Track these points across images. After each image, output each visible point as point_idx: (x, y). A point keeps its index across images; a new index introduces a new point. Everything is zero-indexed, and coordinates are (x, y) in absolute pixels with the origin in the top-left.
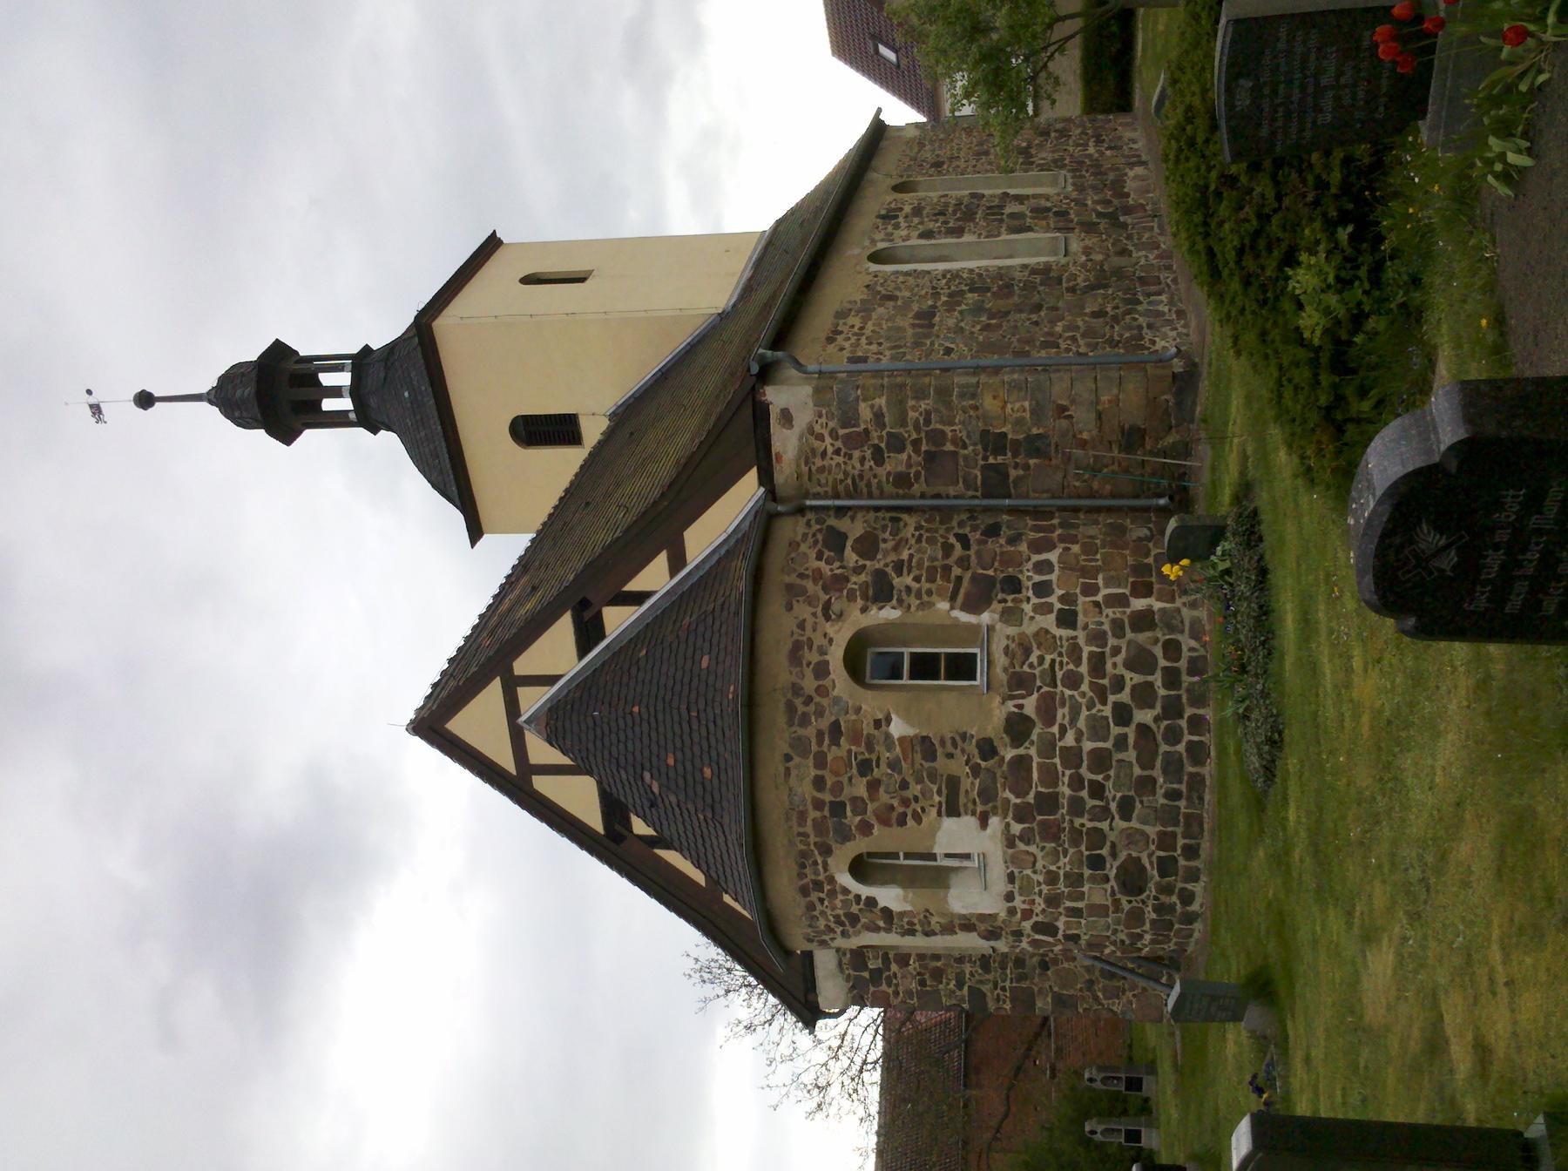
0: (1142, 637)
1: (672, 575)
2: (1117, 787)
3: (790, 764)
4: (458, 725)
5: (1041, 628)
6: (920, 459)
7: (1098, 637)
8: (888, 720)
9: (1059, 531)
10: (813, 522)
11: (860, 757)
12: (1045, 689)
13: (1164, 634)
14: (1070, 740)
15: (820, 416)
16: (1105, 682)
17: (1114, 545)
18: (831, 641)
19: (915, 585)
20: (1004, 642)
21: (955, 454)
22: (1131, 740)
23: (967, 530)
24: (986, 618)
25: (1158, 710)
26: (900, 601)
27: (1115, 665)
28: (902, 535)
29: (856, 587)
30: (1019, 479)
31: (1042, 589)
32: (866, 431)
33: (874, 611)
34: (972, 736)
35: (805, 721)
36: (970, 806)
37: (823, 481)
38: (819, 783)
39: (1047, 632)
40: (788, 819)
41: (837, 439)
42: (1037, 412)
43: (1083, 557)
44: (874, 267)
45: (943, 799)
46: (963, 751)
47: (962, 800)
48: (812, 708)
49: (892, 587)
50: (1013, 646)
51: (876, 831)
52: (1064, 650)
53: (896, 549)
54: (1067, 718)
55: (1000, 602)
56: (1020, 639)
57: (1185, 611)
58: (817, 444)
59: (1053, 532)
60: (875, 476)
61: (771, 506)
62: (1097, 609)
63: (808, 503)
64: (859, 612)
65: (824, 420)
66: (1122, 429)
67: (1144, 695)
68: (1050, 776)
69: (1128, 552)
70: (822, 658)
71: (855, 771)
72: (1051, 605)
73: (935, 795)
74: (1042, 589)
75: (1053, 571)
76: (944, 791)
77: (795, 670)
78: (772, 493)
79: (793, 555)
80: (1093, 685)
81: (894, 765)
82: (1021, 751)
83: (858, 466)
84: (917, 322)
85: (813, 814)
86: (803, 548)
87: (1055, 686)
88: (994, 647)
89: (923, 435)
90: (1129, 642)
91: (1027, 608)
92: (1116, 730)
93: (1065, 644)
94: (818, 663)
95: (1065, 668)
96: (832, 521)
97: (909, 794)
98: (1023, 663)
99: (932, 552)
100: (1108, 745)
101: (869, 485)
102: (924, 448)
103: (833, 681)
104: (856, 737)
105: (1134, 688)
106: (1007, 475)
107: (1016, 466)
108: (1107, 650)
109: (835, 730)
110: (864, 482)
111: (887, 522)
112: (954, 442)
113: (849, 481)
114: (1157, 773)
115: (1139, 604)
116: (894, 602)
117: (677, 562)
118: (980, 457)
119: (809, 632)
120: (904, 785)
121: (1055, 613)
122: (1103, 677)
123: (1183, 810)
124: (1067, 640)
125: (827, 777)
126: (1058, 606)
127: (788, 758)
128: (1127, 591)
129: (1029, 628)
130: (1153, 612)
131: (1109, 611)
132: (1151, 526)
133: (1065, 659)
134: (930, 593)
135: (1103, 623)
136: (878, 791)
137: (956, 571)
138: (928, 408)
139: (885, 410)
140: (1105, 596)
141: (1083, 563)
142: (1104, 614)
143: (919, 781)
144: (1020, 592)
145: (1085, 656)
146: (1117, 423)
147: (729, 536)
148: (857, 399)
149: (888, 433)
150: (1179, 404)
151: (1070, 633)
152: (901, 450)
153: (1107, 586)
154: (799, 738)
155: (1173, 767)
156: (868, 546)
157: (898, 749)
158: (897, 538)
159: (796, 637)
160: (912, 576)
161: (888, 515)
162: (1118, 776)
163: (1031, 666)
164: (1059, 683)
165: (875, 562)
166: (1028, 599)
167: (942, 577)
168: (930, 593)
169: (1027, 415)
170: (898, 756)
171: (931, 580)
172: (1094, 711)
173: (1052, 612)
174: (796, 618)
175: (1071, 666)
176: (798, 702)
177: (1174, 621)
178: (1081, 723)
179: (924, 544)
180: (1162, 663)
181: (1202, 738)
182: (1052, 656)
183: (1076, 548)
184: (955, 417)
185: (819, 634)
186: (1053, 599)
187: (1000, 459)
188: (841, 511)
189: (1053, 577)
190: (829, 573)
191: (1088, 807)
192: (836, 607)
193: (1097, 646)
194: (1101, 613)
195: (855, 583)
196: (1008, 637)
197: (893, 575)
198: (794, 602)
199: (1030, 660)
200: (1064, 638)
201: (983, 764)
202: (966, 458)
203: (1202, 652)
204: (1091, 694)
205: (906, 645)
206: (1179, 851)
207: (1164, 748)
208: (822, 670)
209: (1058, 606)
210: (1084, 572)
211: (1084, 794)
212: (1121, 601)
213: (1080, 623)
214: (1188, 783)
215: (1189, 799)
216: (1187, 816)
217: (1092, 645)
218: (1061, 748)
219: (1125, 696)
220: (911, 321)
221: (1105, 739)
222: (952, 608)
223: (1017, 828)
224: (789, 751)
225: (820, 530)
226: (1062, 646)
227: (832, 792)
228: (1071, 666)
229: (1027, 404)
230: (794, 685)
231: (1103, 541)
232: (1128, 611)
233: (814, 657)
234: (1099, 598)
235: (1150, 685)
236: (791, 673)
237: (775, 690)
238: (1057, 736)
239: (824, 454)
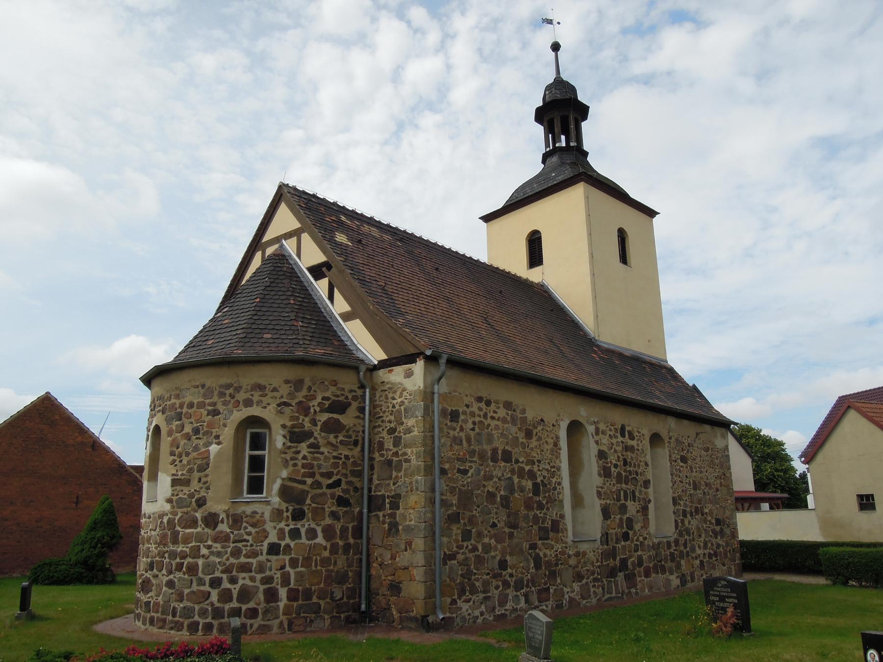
0: (261, 596)
1: (339, 315)
2: (180, 579)
3: (200, 388)
4: (283, 209)
5: (268, 533)
6: (390, 457)
7: (261, 568)
8: (219, 444)
9: (341, 543)
10: (354, 394)
11: (201, 427)
12: (232, 536)
13: (261, 609)
14: (204, 551)
15: (410, 395)
16: (234, 573)
17: (328, 577)
18: (265, 407)
19: (300, 456)
20: (260, 511)
21: (391, 477)
22: (202, 588)
23: (344, 486)
24: (276, 500)
25: (217, 605)
26: (289, 448)
27: (244, 578)
28: (340, 447)
29: (300, 421)
30: (377, 516)
31: (295, 534)
32: (402, 423)
33: (282, 432)
34: (208, 493)
35: (222, 394)
36: (176, 493)
37: (381, 399)
38: (191, 405)
39: (266, 537)
40: (177, 388)
41: (400, 406)
42: (408, 529)
43: (318, 559)
44: (564, 425)
45: (179, 477)
46: (201, 488)
47: (179, 488)
48: (228, 398)
49: (299, 442)
50: (258, 516)
51: (169, 439)
52: (254, 547)
53: (330, 444)
54: (215, 550)
55: (287, 508)
56: (261, 521)
57: (277, 621)
58: (398, 393)
59: (341, 539)
60: (383, 430)
61: (363, 368)
62: (279, 568)
63: (367, 390)
64: (282, 423)
65: (408, 397)
66: (400, 583)
67: (226, 596)
68: (186, 540)
69: (322, 585)
70: (255, 402)
71: (195, 425)
72: (283, 539)
73: (181, 472)
74: (295, 534)
75: (308, 539)
76: (183, 477)
77: (249, 387)
78: (375, 368)
79: (326, 383)
80: (232, 565)
81: (196, 448)
82: (200, 522)
83: (388, 419)
84: (500, 452)
85: (178, 402)
86: (333, 389)
87: (233, 543)
88: (257, 505)
89: (400, 458)
90: (257, 587)
91: (282, 525)
92: (207, 578)
93: (258, 548)
94: (252, 401)
95: (243, 548)
96: (355, 405)
97: (184, 457)
98: (247, 523)
99: (326, 467)
100: (200, 574)
101: (379, 426)
102: (395, 459)
103: (241, 410)
104: (211, 425)
105: (229, 590)
106: (380, 511)
107: (384, 516)
108: (253, 574)
109: (215, 413)
110: (381, 424)
111: (354, 438)
112: (397, 477)
113: (381, 414)
114: (186, 603)
115: (283, 593)
116: (289, 444)
117: (347, 317)
118: (389, 494)
119: (271, 394)
120: (187, 454)
121: (278, 542)
122: (237, 572)
123: (168, 617)
124: (260, 550)
125: (193, 410)
126: (283, 543)
127: (203, 386)
128: (292, 586)
129: (269, 526)
130: (278, 601)
131: (278, 575)
132: (345, 600)
133: (248, 548)
134: (295, 465)
135: (271, 571)
136: (185, 439)
137: (309, 481)
138: (412, 461)
139: (412, 434)
140: (289, 573)
141: (314, 558)
142: (277, 572)
143: (189, 463)
144: (293, 520)
145: (250, 560)
146: (403, 579)
147: (356, 345)
148: (417, 417)
149: (402, 436)
150: (411, 619)
151: (265, 552)
152: (394, 446)
153: (296, 573)
154: (212, 392)
155: (188, 613)
156: (331, 427)
157: (204, 450)
158: (338, 444)
159: (268, 386)
160: (306, 454)
161: (360, 439)
162: (184, 579)
163: (246, 528)
164: (235, 545)
165: (319, 432)
166: (288, 525)
167: (305, 472)
168: (295, 465)
169: (408, 523)
170: (200, 450)
171: (304, 466)
172: (218, 566)
173: (279, 539)
174: (280, 387)
175: (244, 552)
176: (231, 390)
177: (270, 614)
178: (213, 559)
179: (332, 461)
180: (244, 607)
181: (200, 631)
182: (250, 540)
183: (326, 554)
184: (408, 478)
185: (270, 401)
186: (288, 540)
187: (388, 506)
188: (362, 410)
189: (304, 540)
190: (311, 405)
191: (172, 562)
192: (287, 410)
193: (255, 567)
194: (277, 570)
195: (303, 420)
196: (263, 513)
197: (308, 443)
198: (290, 385)
199: (249, 527)
200: (261, 547)
201: (194, 500)
202: (389, 484)
203: (250, 632)
204: (228, 564)
205: (269, 452)
206: (152, 614)
207: (197, 607)
208: (248, 403)
209: (283, 543)
210: (307, 561)
211: (178, 560)
212: (286, 581)
213: (270, 557)
214: (179, 621)
215: (172, 622)
216: (166, 619)
217: (256, 565)
218: (200, 546)
219: (226, 585)
220: (501, 448)
221: (203, 572)
222: (283, 479)
223: (165, 520)
224: (207, 387)
225: (347, 398)
226: (256, 546)
227: (187, 413)
228: (244, 552)
229: (413, 523)
230: (241, 387)
231: (332, 571)
232: (279, 587)
233: (256, 398)
234: (288, 568)
235: (231, 600)
236: (247, 385)
237: (238, 376)
238: (205, 544)
239: (394, 399)
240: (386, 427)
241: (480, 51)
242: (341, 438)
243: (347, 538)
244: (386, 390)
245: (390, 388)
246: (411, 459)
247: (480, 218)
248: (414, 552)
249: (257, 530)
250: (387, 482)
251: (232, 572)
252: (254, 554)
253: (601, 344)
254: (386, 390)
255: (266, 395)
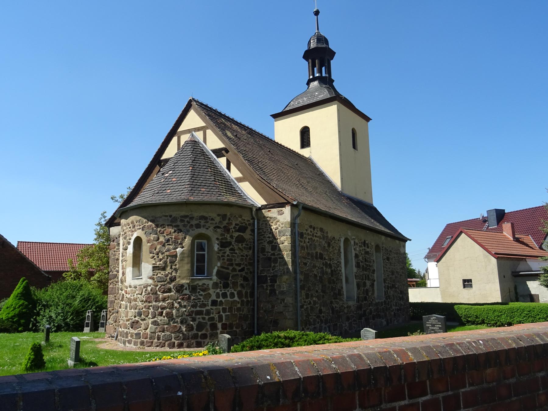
0: (208, 327)
5: (211, 295)
8: (182, 248)
16: (194, 316)
18: (207, 229)
19: (226, 254)
20: (207, 284)
21: (271, 266)
23: (246, 270)
24: (215, 278)
26: (220, 250)
27: (199, 318)
33: (217, 242)
39: (210, 297)
43: (236, 308)
48: (186, 223)
49: (226, 247)
55: (220, 282)
60: (264, 242)
62: (217, 313)
65: (281, 225)
69: (238, 321)
74: (224, 295)
86: (240, 219)
89: (276, 256)
90: (206, 323)
91: (218, 290)
93: (206, 303)
94: (200, 225)
95: (198, 303)
96: (250, 228)
99: (238, 261)
101: (262, 239)
102: (273, 257)
103: (194, 230)
106: (264, 283)
107: (267, 286)
110: (263, 238)
112: (274, 266)
113: (263, 233)
115: (219, 325)
116: (220, 248)
118: (270, 275)
119: (210, 222)
122: (195, 315)
126: (219, 300)
128: (224, 322)
129: (211, 291)
133: (201, 303)
137: (231, 268)
140: (222, 315)
142: (216, 315)
144: (224, 288)
145: (202, 309)
153: (226, 316)
154: (177, 220)
156: (240, 240)
158: (243, 249)
160: (229, 254)
161: (252, 246)
163: (199, 292)
166: (221, 291)
169: (282, 289)
173: (217, 298)
174: (215, 218)
175: (199, 305)
176: (188, 219)
179: (241, 257)
180: (200, 333)
183: (239, 305)
186: (221, 299)
187: (269, 281)
188: (253, 231)
189: (229, 299)
192: (218, 230)
194: (216, 314)
196: (208, 284)
197: (230, 248)
198: (220, 217)
201: (168, 278)
202: (269, 270)
208: (198, 226)
210: (230, 309)
213: (212, 307)
222: (218, 267)
224: (173, 217)
225: (246, 224)
226: (205, 301)
228: (199, 305)
229: (285, 289)
243: (248, 298)
249: (205, 293)
250: (269, 269)
251: (192, 315)
252: (204, 305)
255: (208, 222)
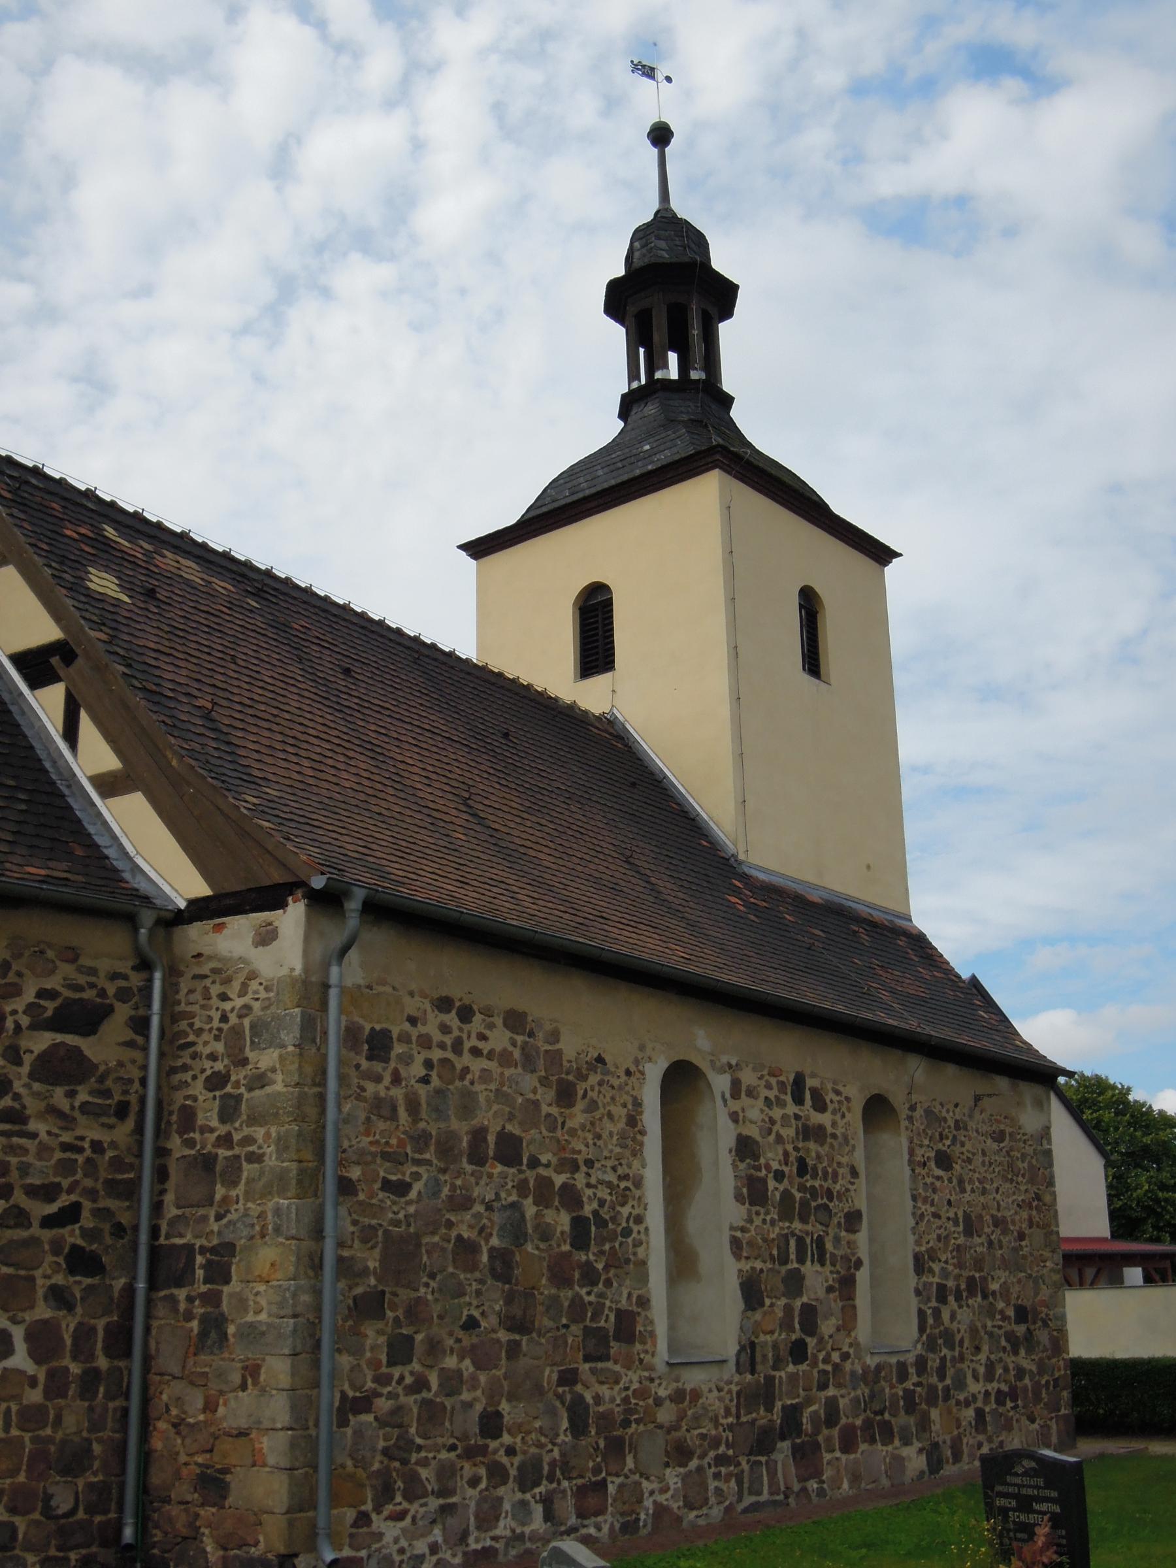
1: (94, 780)
6: (209, 1146)
9: (75, 1369)
10: (122, 983)
15: (267, 989)
23: (87, 1220)
28: (82, 1119)
30: (173, 1300)
32: (244, 1062)
37: (192, 998)
41: (240, 1017)
42: (251, 1333)
43: (14, 1408)
44: (654, 1072)
53: (53, 1111)
58: (236, 985)
59: (74, 1358)
60: (194, 1077)
61: (147, 918)
63: (158, 975)
65: (263, 995)
66: (226, 1471)
69: (22, 1478)
78: (180, 918)
79: (50, 954)
83: (207, 1051)
84: (491, 1139)
86: (66, 969)
89: (237, 1151)
96: (123, 1012)
99: (42, 1171)
101: (185, 1068)
102: (223, 1153)
106: (179, 1284)
107: (190, 1299)
110: (189, 1061)
111: (117, 1097)
112: (225, 1200)
113: (191, 1038)
117: (109, 785)
132: (81, 1515)
138: (266, 1158)
147: (130, 859)
149: (241, 1095)
158: (77, 1114)
161: (133, 1099)
165: (25, 1080)
169: (250, 1318)
179: (59, 1155)
184: (254, 1201)
187: (200, 1273)
188: (141, 1025)
190: (8, 1009)
202: (205, 1218)
220: (494, 1129)
225: (102, 993)
229: (263, 1317)
231: (50, 1440)
239: (224, 997)
240: (203, 1071)
241: (498, 109)
242: (83, 1096)
243: (92, 1356)
244: (206, 977)
245: (215, 971)
246: (263, 1154)
247: (461, 547)
248: (263, 1391)
250: (201, 1211)
253: (754, 873)
254: (206, 977)
